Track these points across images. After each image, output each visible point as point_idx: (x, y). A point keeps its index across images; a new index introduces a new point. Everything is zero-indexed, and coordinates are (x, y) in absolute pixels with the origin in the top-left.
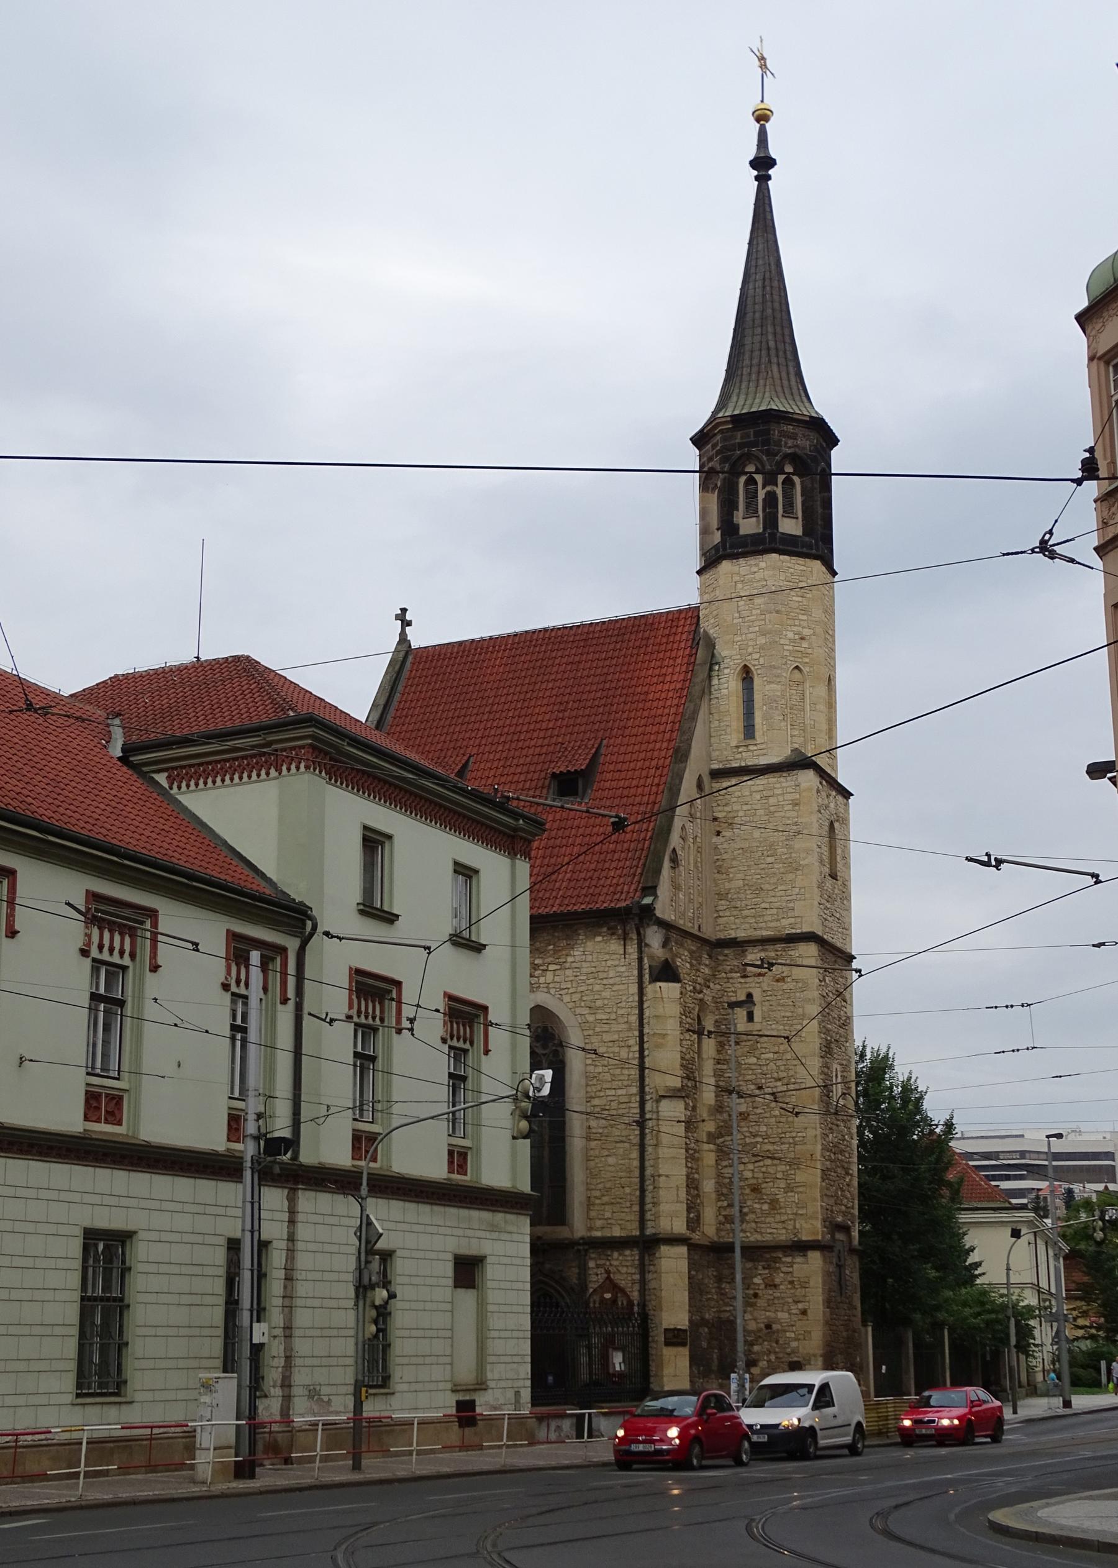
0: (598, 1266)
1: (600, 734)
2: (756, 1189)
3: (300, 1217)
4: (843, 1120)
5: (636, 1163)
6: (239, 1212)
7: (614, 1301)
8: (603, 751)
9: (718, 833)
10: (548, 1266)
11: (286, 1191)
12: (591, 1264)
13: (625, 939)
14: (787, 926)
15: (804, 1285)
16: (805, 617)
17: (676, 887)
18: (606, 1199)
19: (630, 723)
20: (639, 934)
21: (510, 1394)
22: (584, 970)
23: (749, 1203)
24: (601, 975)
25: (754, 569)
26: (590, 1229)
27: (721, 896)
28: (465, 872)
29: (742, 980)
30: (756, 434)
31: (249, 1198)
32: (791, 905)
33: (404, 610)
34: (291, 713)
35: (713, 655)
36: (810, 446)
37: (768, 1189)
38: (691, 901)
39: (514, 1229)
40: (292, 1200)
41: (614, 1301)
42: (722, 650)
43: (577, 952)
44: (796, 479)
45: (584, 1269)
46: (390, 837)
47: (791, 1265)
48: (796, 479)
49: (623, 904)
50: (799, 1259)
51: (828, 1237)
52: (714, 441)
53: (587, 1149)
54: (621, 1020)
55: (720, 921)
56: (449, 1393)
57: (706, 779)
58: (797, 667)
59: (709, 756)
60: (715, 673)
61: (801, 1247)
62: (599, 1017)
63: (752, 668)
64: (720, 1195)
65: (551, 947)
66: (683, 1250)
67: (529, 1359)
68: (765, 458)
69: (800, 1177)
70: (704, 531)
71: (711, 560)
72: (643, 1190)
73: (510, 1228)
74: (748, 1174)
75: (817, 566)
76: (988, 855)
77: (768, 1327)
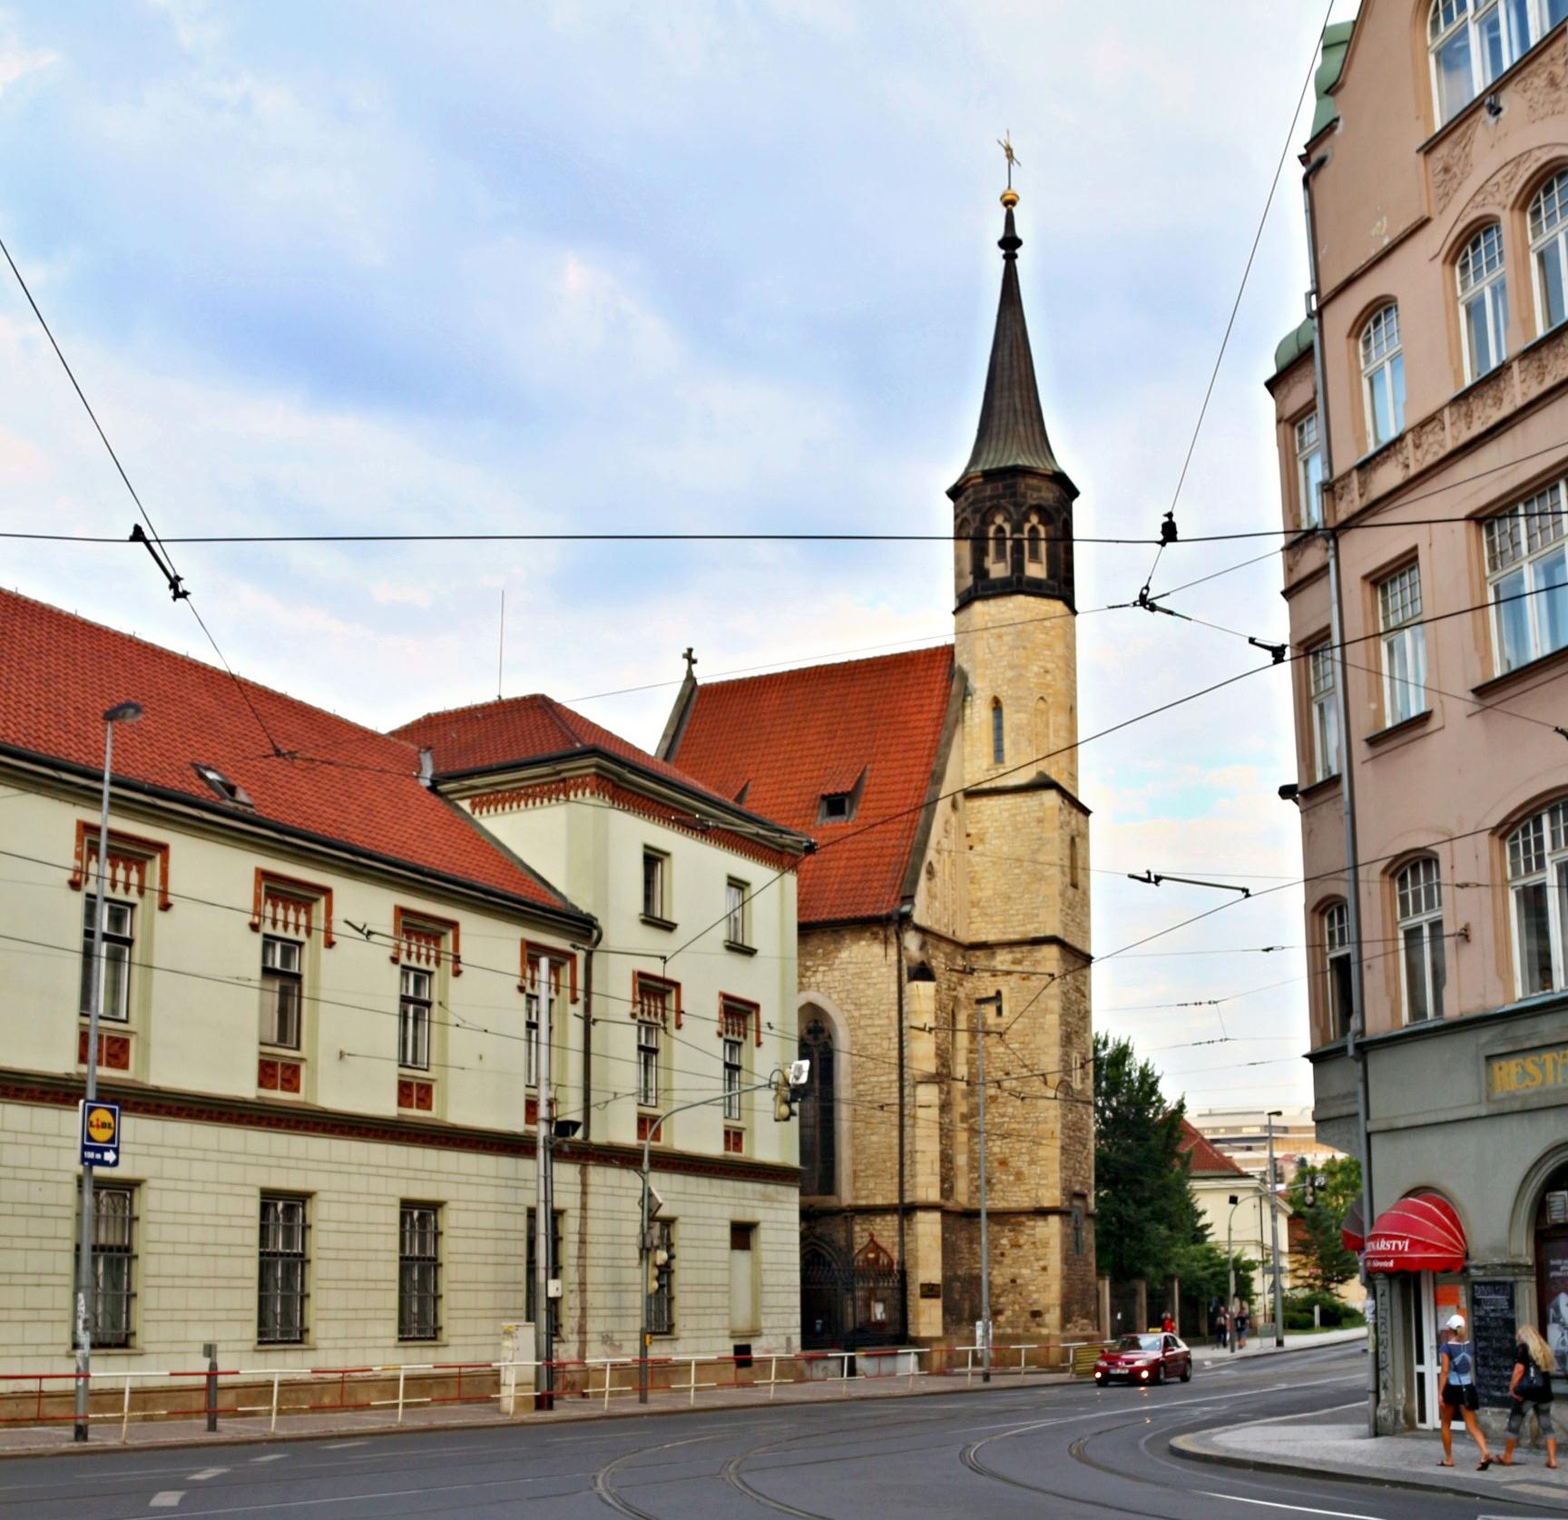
0: (863, 1230)
1: (866, 759)
2: (1003, 1163)
3: (591, 1189)
5: (896, 1141)
6: (534, 1185)
7: (877, 1259)
8: (867, 774)
9: (971, 848)
10: (818, 1230)
11: (578, 1168)
12: (857, 1228)
13: (886, 943)
14: (1033, 931)
15: (1045, 1245)
16: (1047, 653)
17: (932, 896)
18: (870, 1172)
19: (893, 749)
20: (898, 938)
21: (782, 1341)
22: (850, 971)
23: (998, 1175)
24: (865, 975)
25: (1003, 609)
26: (856, 1198)
27: (974, 904)
28: (737, 884)
30: (1005, 487)
31: (542, 1172)
33: (690, 650)
34: (578, 745)
35: (966, 688)
37: (1015, 1163)
38: (946, 909)
39: (784, 1198)
40: (583, 1174)
41: (877, 1259)
42: (976, 683)
43: (844, 955)
44: (1042, 529)
45: (850, 1233)
46: (667, 854)
47: (1033, 1228)
48: (1042, 529)
49: (884, 912)
50: (1040, 1223)
51: (1067, 1203)
52: (966, 494)
53: (853, 1129)
54: (883, 1015)
55: (973, 926)
56: (727, 1339)
58: (1042, 698)
59: (963, 781)
60: (967, 704)
61: (1042, 1213)
62: (864, 1012)
63: (1002, 700)
65: (820, 951)
66: (937, 1216)
67: (798, 1310)
68: (1012, 509)
69: (1042, 1152)
70: (959, 575)
71: (965, 601)
72: (902, 1165)
73: (781, 1198)
74: (996, 1150)
75: (1058, 607)
76: (1149, 873)
77: (1013, 1281)
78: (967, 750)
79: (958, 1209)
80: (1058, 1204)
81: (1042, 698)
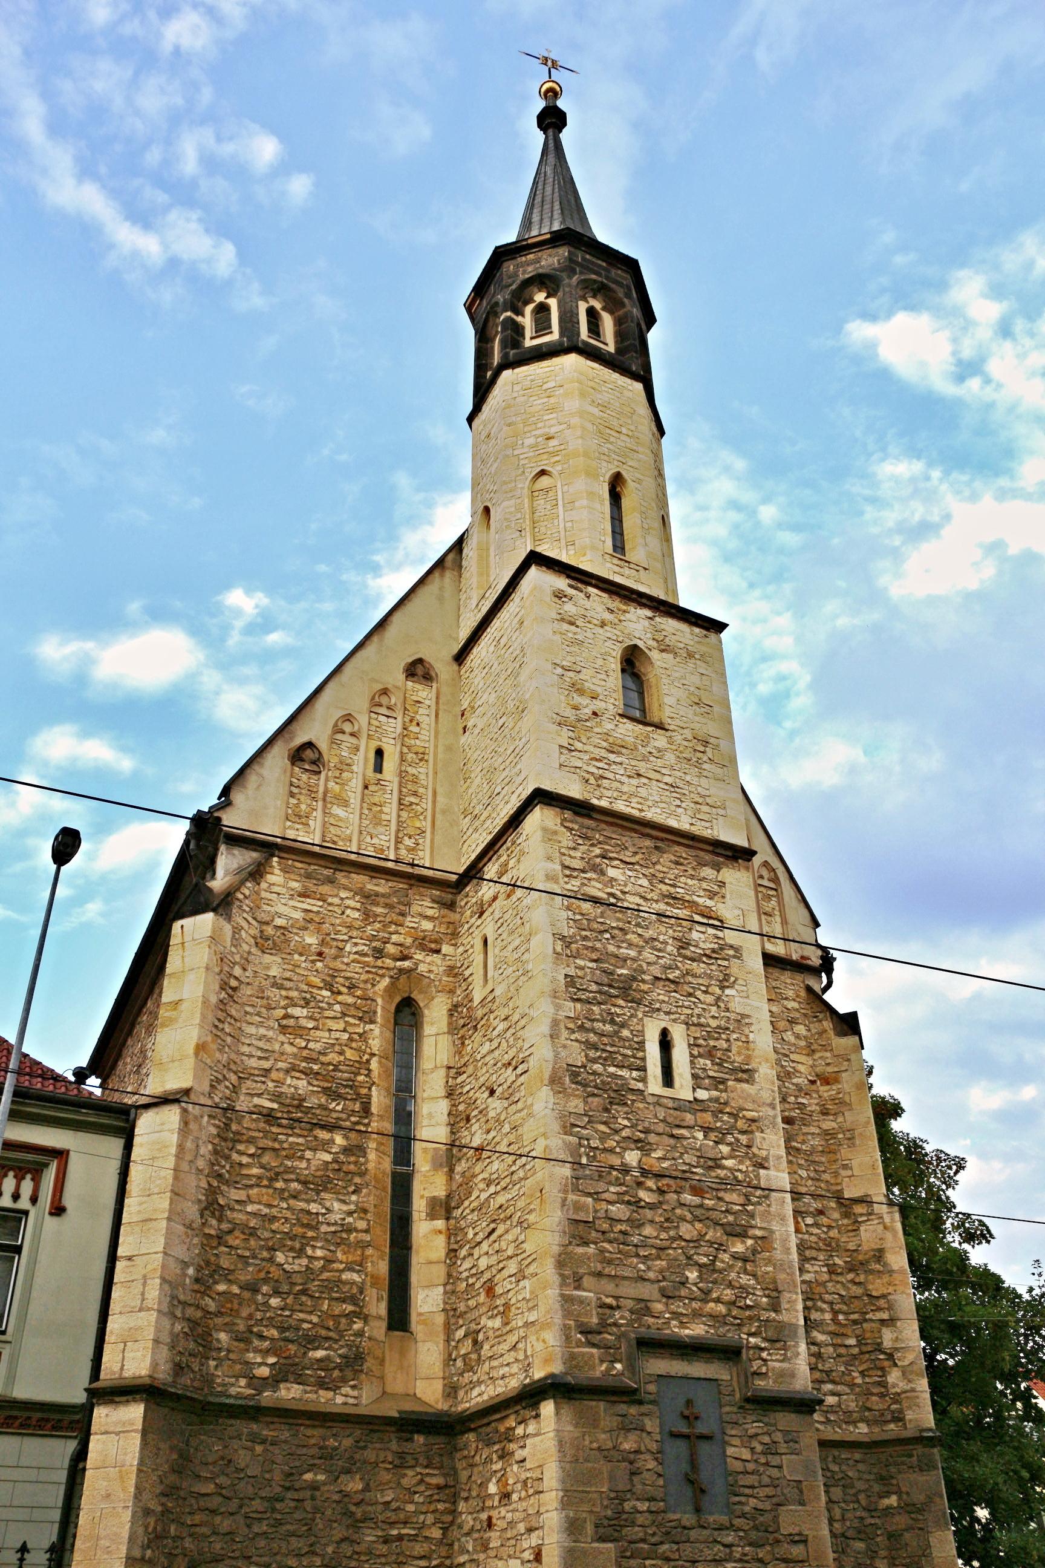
4: (707, 1130)
29: (479, 922)
32: (519, 767)
36: (559, 261)
48: (553, 303)
57: (442, 665)
58: (543, 473)
64: (452, 1314)
78: (463, 597)
79: (391, 1411)
80: (557, 1368)
81: (543, 473)
